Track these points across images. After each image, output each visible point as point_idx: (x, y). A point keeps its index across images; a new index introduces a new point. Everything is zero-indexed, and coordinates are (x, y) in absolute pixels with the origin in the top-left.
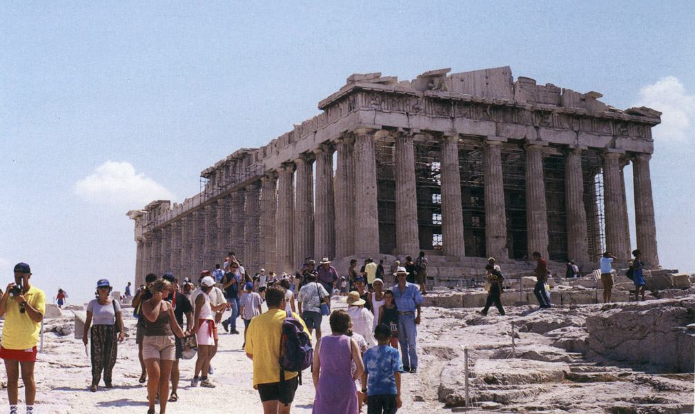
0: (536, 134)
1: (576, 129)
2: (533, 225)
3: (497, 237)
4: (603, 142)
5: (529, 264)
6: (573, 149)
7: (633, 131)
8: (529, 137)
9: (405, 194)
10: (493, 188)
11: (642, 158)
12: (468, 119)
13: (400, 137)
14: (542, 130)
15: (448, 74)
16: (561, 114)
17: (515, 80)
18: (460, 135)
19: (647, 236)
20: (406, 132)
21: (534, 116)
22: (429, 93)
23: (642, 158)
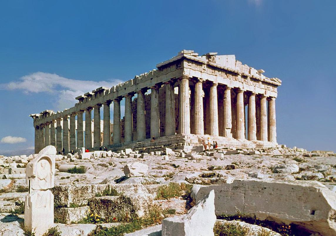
4: (262, 92)
6: (253, 93)
8: (240, 87)
18: (218, 83)
20: (200, 80)
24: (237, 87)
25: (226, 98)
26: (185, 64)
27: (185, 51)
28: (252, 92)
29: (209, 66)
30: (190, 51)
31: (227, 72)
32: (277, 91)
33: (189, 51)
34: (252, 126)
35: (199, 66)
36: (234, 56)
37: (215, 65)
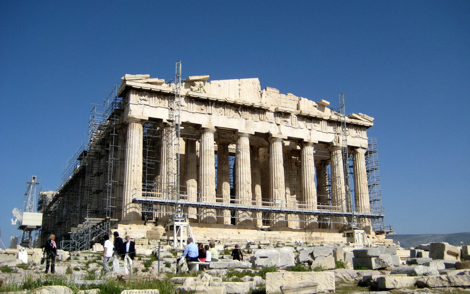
4: (329, 138)
8: (271, 132)
14: (283, 127)
18: (216, 127)
20: (170, 123)
21: (276, 115)
24: (264, 131)
26: (134, 98)
27: (128, 76)
28: (302, 139)
29: (190, 99)
30: (139, 76)
31: (237, 107)
32: (368, 136)
33: (137, 76)
35: (154, 98)
36: (256, 80)
37: (203, 96)
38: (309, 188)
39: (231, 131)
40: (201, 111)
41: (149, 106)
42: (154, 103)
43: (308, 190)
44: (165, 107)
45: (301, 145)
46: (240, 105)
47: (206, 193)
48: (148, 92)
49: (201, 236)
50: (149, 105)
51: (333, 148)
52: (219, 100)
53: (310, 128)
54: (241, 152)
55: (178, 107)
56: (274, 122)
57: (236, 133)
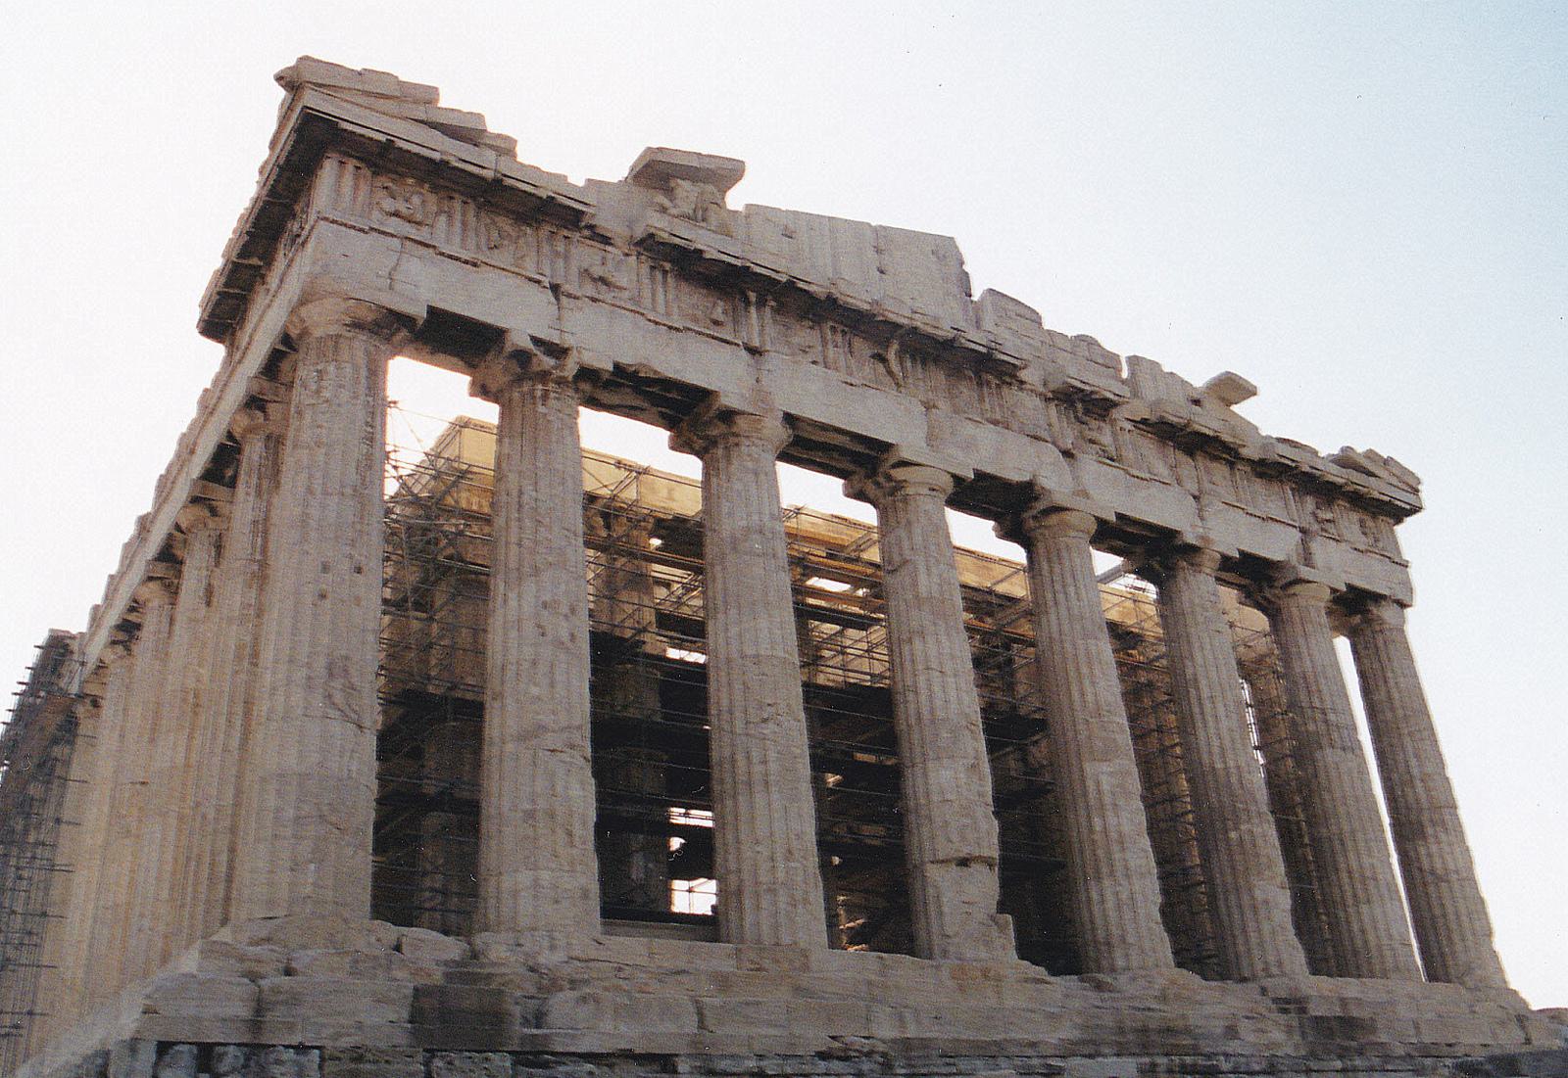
0: (1068, 478)
1: (1194, 488)
2: (1097, 823)
3: (964, 862)
4: (1276, 545)
5: (1099, 987)
7: (1349, 522)
9: (529, 628)
10: (933, 652)
11: (1387, 613)
12: (819, 369)
13: (519, 380)
15: (736, 199)
16: (1142, 425)
17: (976, 297)
18: (790, 419)
19: (1455, 876)
20: (548, 362)
21: (1053, 410)
22: (661, 225)
23: (1387, 613)
25: (905, 562)
34: (1233, 835)
38: (1238, 767)
39: (857, 458)
40: (712, 326)
41: (431, 250)
42: (457, 239)
43: (1234, 780)
44: (517, 270)
45: (1161, 564)
46: (897, 326)
47: (765, 762)
48: (427, 186)
49: (770, 1024)
50: (434, 247)
51: (1291, 591)
52: (801, 285)
53: (1197, 493)
54: (920, 562)
55: (589, 289)
56: (1044, 435)
57: (885, 467)
